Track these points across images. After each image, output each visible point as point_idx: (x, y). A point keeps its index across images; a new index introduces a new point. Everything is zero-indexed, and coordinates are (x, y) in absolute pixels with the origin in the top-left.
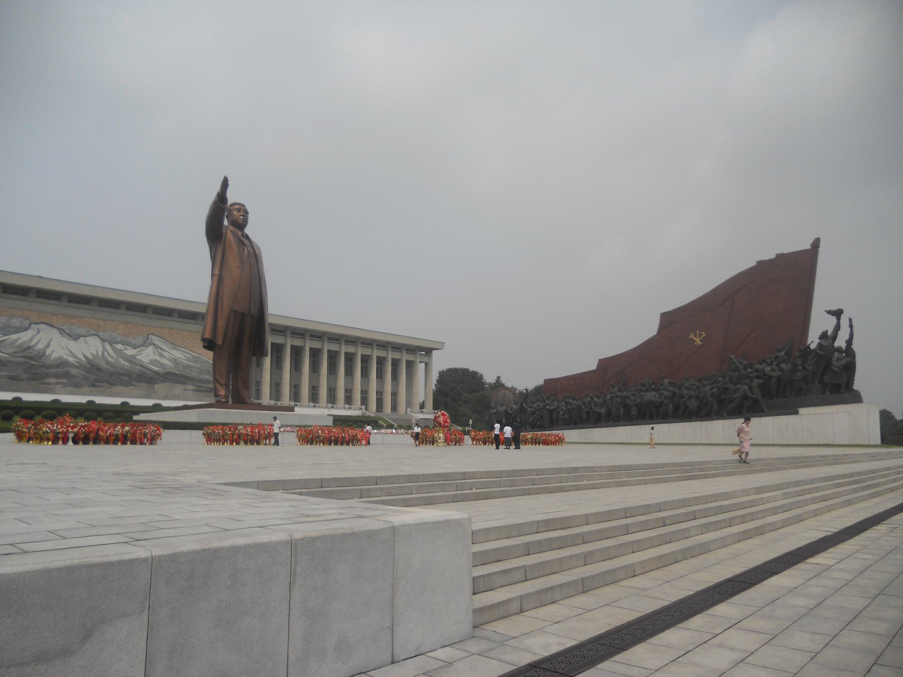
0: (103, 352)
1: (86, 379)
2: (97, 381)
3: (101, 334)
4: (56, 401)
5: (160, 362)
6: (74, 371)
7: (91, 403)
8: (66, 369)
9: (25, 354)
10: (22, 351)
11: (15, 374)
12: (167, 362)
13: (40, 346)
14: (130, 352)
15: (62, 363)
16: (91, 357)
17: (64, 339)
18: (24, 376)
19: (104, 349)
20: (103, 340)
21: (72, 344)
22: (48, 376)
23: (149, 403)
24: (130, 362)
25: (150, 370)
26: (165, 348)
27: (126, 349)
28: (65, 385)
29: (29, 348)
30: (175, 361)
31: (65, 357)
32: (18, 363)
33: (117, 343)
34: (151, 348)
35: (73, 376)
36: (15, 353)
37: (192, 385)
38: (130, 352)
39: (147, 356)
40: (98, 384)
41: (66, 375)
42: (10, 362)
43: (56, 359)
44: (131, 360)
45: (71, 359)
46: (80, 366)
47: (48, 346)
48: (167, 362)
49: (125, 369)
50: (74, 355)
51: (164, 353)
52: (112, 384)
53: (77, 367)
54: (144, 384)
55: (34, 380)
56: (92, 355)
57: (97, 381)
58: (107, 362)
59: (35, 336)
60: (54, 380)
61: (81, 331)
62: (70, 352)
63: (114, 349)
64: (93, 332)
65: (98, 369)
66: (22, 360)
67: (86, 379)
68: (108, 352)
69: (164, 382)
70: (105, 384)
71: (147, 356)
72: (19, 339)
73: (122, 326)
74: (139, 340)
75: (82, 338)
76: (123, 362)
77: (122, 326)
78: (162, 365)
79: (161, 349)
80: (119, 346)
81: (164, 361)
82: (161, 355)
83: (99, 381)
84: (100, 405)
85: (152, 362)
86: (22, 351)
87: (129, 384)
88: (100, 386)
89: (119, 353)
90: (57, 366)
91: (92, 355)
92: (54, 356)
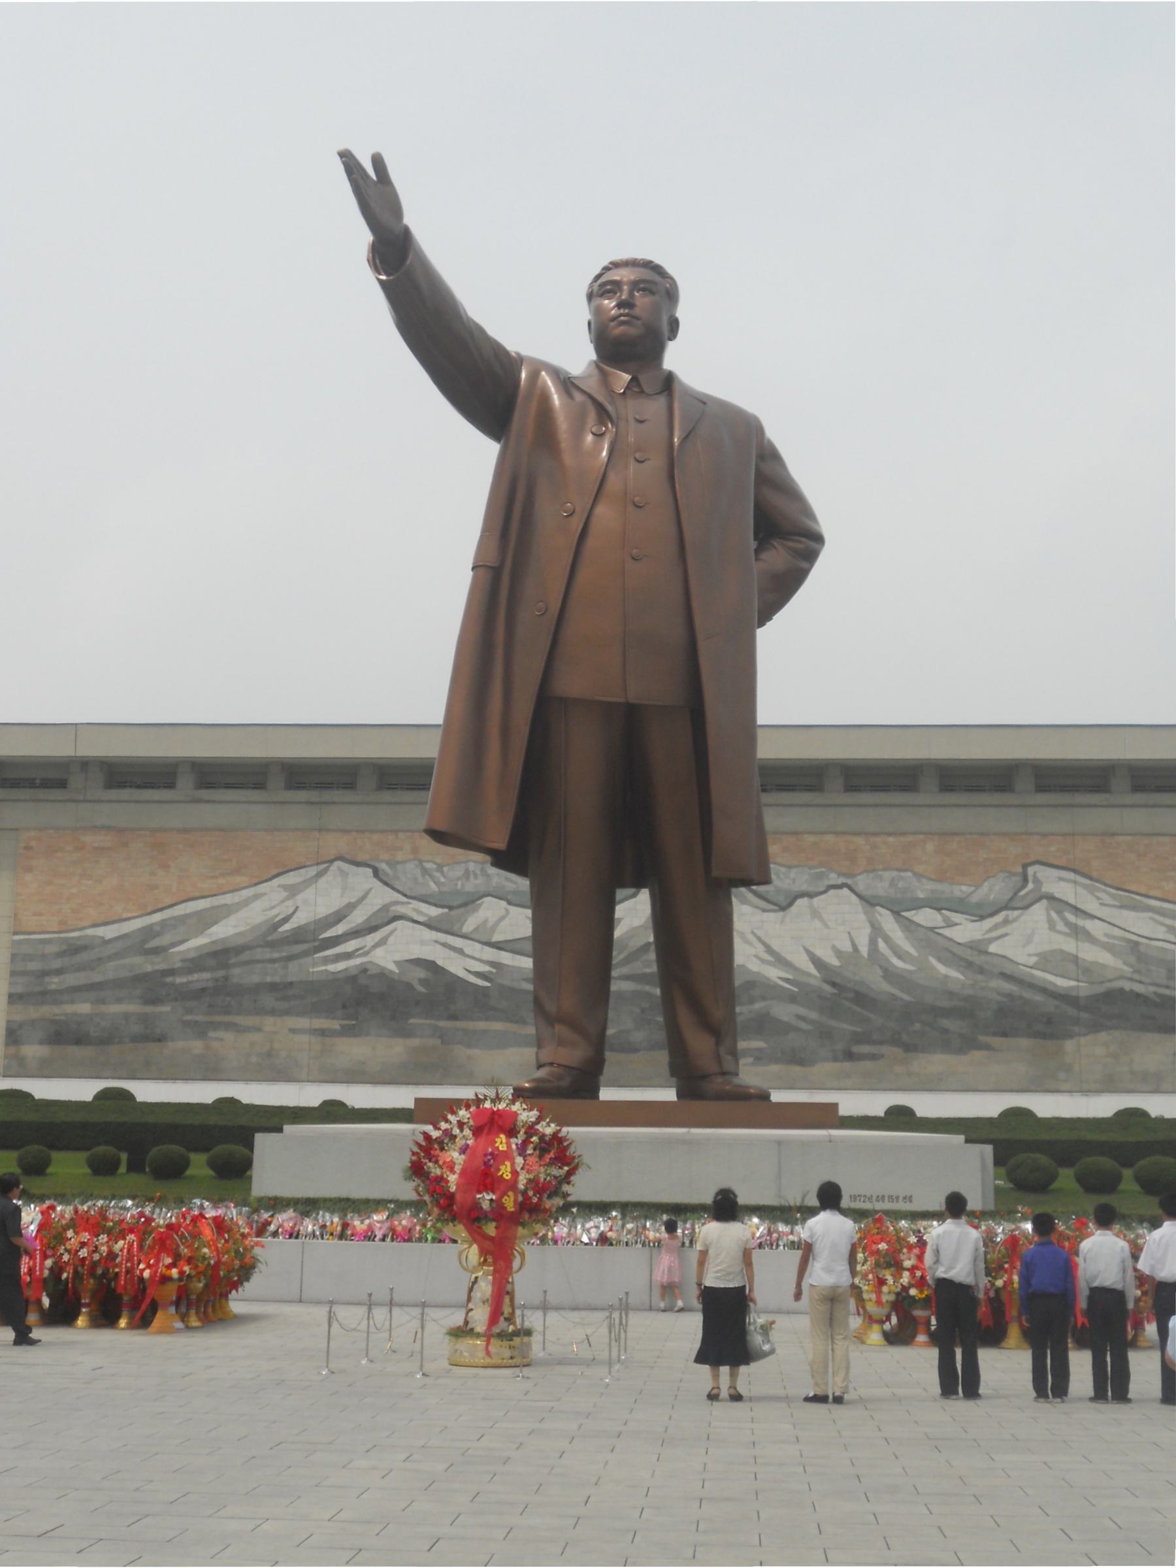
0: (873, 943)
1: (825, 1034)
2: (858, 1039)
4: (229, 1104)
5: (1075, 959)
6: (784, 1012)
7: (221, 1102)
8: (758, 1006)
12: (1105, 958)
14: (965, 931)
16: (835, 962)
18: (638, 1037)
19: (877, 931)
20: (869, 902)
23: (311, 1095)
24: (969, 965)
25: (1044, 990)
26: (1091, 906)
27: (951, 924)
30: (1134, 949)
33: (918, 905)
34: (1039, 912)
35: (787, 1028)
38: (965, 931)
39: (1029, 940)
40: (865, 1049)
44: (972, 959)
45: (774, 974)
46: (800, 994)
48: (1105, 958)
49: (951, 994)
50: (780, 960)
51: (1089, 925)
52: (909, 1048)
53: (793, 999)
54: (1024, 1042)
56: (838, 953)
57: (858, 1039)
58: (889, 974)
62: (769, 949)
63: (909, 927)
64: (834, 879)
65: (862, 998)
67: (825, 1034)
68: (887, 940)
69: (1095, 1027)
70: (886, 1050)
71: (1026, 942)
73: (930, 847)
74: (994, 889)
75: (802, 902)
76: (942, 969)
77: (930, 847)
78: (1085, 969)
79: (1077, 910)
80: (926, 917)
81: (1090, 953)
82: (1077, 932)
84: (1161, 1120)
85: (1046, 960)
87: (968, 1044)
88: (873, 1057)
89: (928, 939)
91: (838, 953)
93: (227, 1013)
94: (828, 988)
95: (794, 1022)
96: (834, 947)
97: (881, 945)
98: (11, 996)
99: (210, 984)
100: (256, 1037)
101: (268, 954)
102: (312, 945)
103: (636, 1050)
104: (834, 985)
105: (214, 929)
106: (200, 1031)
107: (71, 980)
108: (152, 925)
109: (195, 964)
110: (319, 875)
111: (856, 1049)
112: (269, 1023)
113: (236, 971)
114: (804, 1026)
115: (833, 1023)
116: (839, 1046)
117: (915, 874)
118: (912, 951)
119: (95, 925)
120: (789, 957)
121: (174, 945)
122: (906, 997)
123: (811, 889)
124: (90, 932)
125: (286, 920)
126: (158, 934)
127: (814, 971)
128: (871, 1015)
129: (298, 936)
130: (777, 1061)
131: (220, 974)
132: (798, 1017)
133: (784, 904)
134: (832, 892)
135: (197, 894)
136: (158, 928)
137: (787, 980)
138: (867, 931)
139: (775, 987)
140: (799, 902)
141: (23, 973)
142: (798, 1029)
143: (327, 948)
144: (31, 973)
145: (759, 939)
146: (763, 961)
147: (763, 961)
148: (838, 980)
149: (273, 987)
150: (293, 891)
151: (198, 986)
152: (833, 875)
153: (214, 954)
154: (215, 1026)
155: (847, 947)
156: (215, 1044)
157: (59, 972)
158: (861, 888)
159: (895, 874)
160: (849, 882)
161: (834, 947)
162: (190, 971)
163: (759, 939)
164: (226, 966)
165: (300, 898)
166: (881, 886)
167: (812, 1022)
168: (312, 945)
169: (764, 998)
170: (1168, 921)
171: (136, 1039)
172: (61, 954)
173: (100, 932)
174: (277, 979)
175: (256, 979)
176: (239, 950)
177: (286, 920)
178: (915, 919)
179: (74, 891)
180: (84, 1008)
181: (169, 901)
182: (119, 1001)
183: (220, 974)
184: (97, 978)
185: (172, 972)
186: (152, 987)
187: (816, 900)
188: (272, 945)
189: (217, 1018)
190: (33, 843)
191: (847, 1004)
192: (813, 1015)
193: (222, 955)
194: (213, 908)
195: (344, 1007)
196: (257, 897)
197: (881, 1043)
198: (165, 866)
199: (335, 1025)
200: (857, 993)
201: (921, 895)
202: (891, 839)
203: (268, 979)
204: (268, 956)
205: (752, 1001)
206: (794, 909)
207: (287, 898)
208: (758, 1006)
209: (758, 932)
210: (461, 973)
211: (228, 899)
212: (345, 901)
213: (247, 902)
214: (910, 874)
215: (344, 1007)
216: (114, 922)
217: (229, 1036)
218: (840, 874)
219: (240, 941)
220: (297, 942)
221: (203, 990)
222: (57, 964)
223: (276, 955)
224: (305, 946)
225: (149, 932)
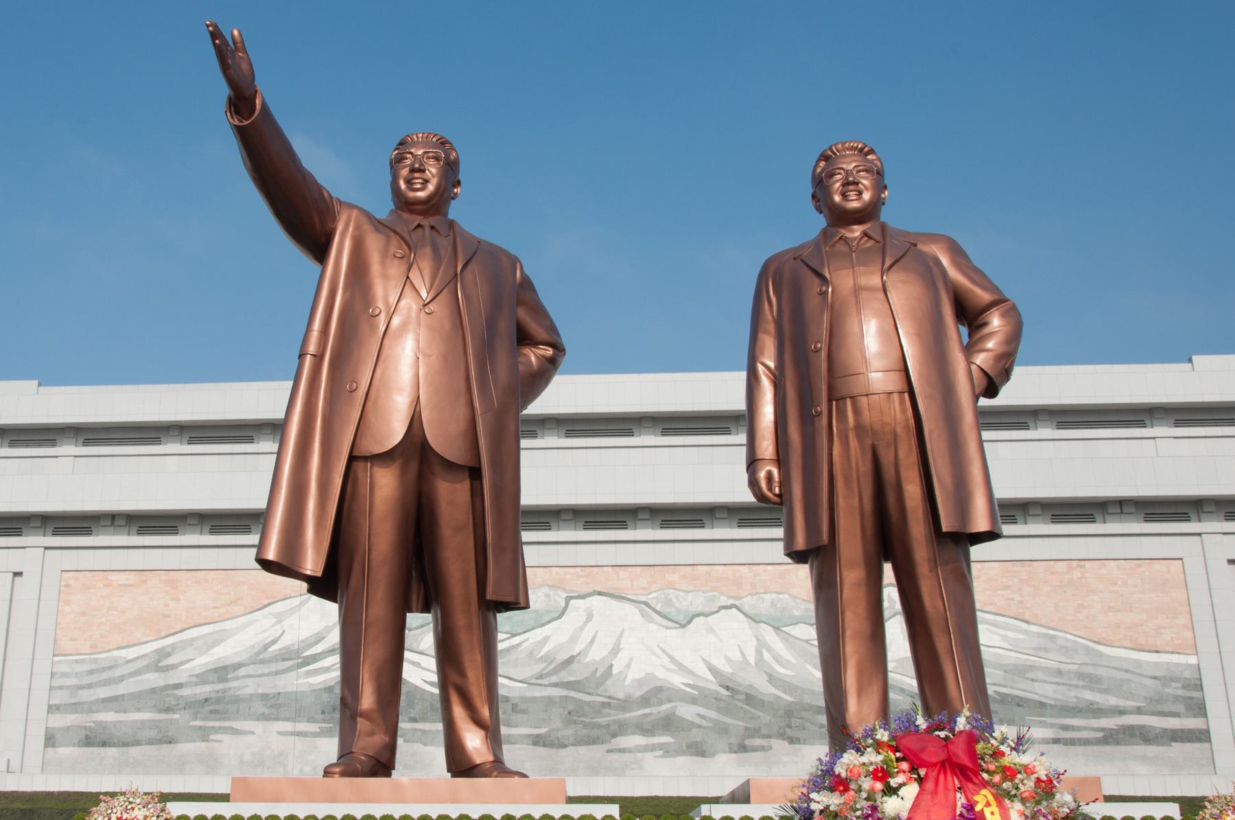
0: (759, 652)
1: (723, 730)
3: (748, 603)
6: (687, 712)
8: (665, 707)
9: (566, 676)
10: (556, 670)
11: (543, 731)
13: (597, 654)
15: (656, 693)
16: (727, 669)
17: (652, 627)
19: (761, 645)
20: (754, 619)
21: (673, 637)
22: (620, 729)
28: (667, 751)
29: (570, 661)
31: (661, 674)
32: (550, 700)
36: (541, 677)
37: (1043, 724)
40: (757, 742)
41: (668, 723)
42: (534, 700)
43: (640, 682)
45: (678, 680)
46: (700, 697)
47: (616, 651)
50: (682, 668)
53: (693, 701)
55: (593, 741)
58: (772, 679)
59: (582, 628)
60: (638, 740)
61: (696, 601)
62: (673, 660)
63: (787, 638)
64: (724, 600)
65: (750, 699)
66: (556, 692)
67: (723, 730)
68: (770, 650)
72: (546, 639)
83: (753, 733)
86: (556, 670)
88: (763, 748)
90: (645, 701)
92: (634, 674)
93: (224, 719)
94: (724, 692)
95: (697, 720)
96: (727, 658)
97: (766, 655)
98: (50, 707)
99: (214, 695)
100: (250, 738)
101: (260, 669)
102: (295, 662)
103: (565, 746)
104: (728, 688)
105: (215, 650)
106: (204, 735)
107: (103, 692)
108: (163, 648)
109: (202, 678)
110: (301, 605)
111: (747, 742)
112: (258, 727)
113: (234, 684)
114: (704, 723)
115: (728, 720)
116: (734, 740)
117: (791, 595)
118: (793, 661)
119: (119, 648)
120: (689, 666)
121: (183, 663)
122: (790, 699)
123: (706, 610)
124: (115, 653)
125: (274, 642)
126: (169, 655)
127: (710, 677)
128: (760, 713)
129: (285, 655)
130: (683, 753)
131: (220, 686)
132: (698, 715)
133: (684, 622)
134: (723, 611)
135: (202, 621)
136: (170, 650)
137: (688, 685)
138: (755, 642)
139: (678, 691)
140: (696, 620)
141: (60, 688)
142: (700, 726)
143: (308, 664)
144: (68, 687)
145: (664, 651)
146: (668, 670)
147: (668, 670)
148: (731, 685)
149: (264, 697)
150: (280, 618)
151: (203, 697)
152: (723, 598)
153: (215, 670)
154: (216, 730)
155: (737, 656)
156: (216, 744)
157: (89, 686)
158: (746, 608)
159: (774, 596)
160: (737, 603)
161: (727, 658)
162: (196, 684)
163: (664, 651)
164: (224, 680)
165: (286, 623)
166: (763, 604)
167: (712, 720)
168: (295, 662)
169: (670, 701)
170: (1001, 632)
171: (151, 742)
172: (91, 672)
173: (124, 653)
174: (266, 691)
175: (249, 691)
176: (239, 666)
177: (274, 642)
178: (792, 633)
179: (103, 620)
180: (109, 717)
181: (179, 628)
182: (139, 710)
183: (220, 686)
184: (120, 690)
185: (179, 686)
186: (163, 699)
187: (710, 618)
188: (262, 662)
189: (217, 724)
190: (72, 582)
191: (740, 704)
192: (713, 714)
193: (222, 672)
194: (213, 633)
195: (323, 712)
196: (249, 624)
197: (769, 736)
198: (177, 600)
199: (314, 728)
200: (747, 695)
201: (797, 613)
202: (770, 568)
203: (260, 691)
204: (260, 672)
205: (660, 704)
206: (692, 626)
207: (275, 624)
208: (665, 707)
209: (663, 646)
210: (419, 683)
211: (226, 625)
212: (323, 625)
213: (243, 627)
214: (786, 596)
215: (323, 712)
216: (135, 645)
217: (226, 738)
218: (729, 597)
219: (236, 660)
220: (284, 660)
221: (206, 700)
222: (86, 680)
223: (266, 671)
224: (290, 663)
225: (163, 653)
